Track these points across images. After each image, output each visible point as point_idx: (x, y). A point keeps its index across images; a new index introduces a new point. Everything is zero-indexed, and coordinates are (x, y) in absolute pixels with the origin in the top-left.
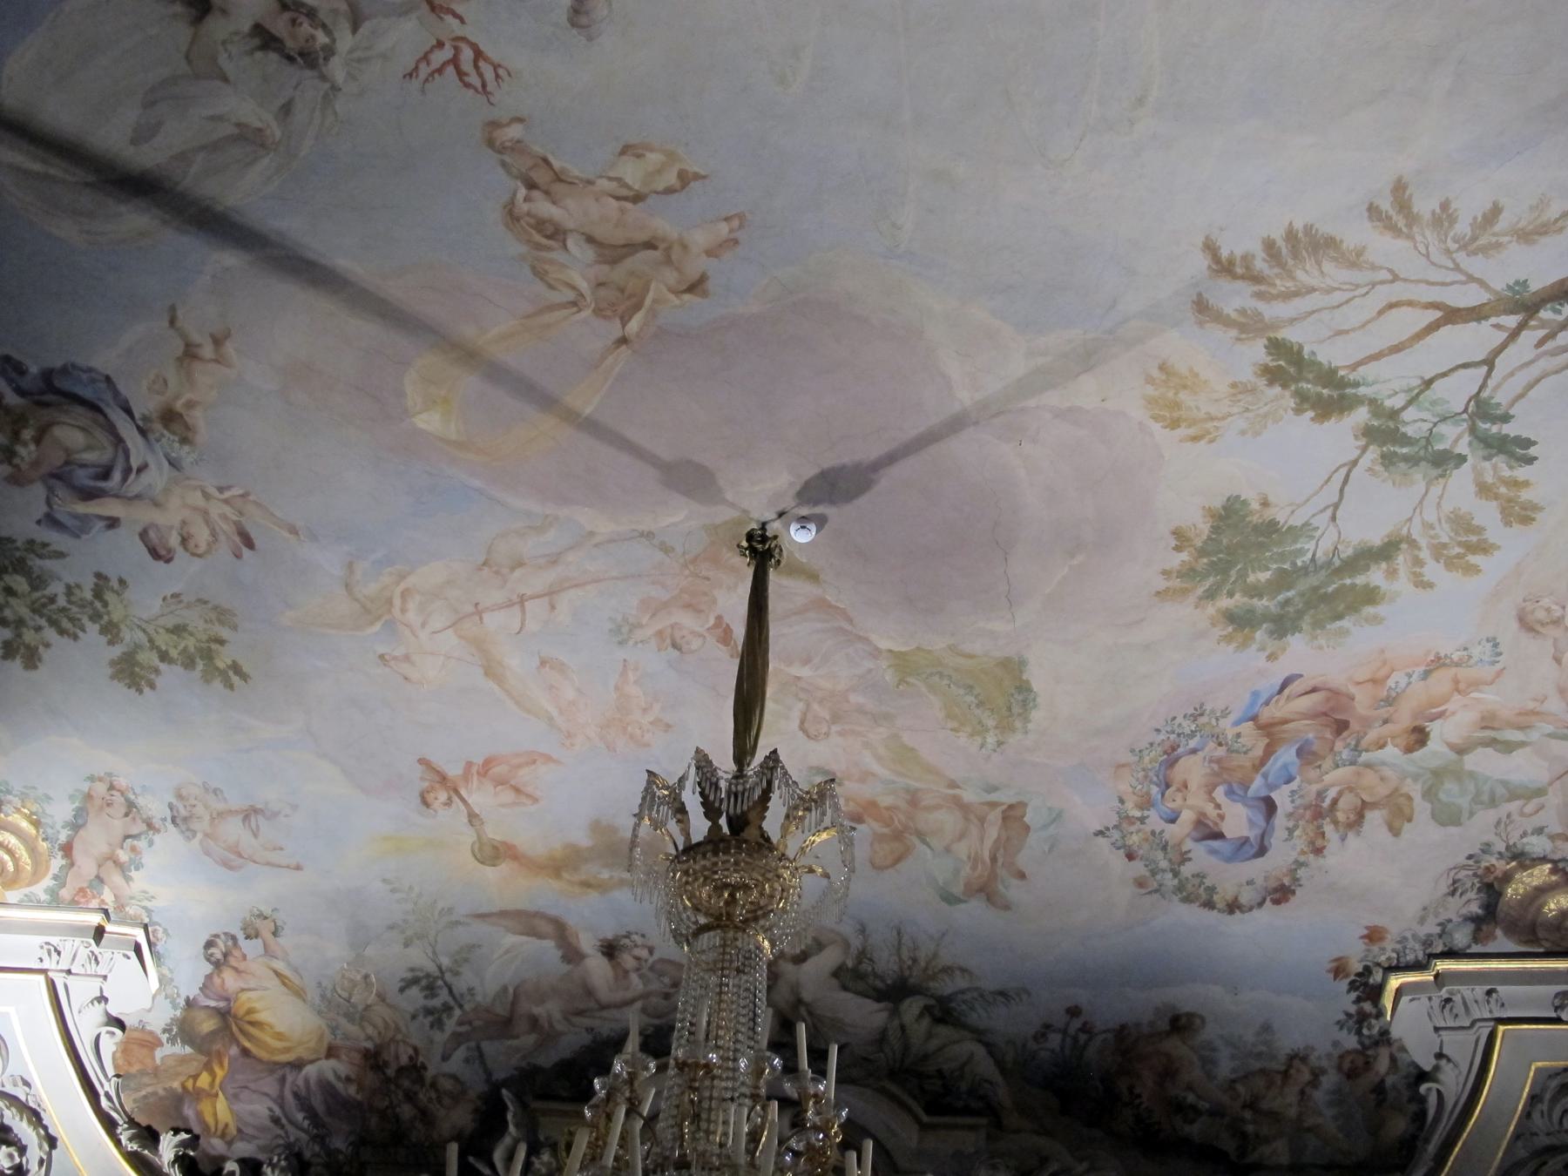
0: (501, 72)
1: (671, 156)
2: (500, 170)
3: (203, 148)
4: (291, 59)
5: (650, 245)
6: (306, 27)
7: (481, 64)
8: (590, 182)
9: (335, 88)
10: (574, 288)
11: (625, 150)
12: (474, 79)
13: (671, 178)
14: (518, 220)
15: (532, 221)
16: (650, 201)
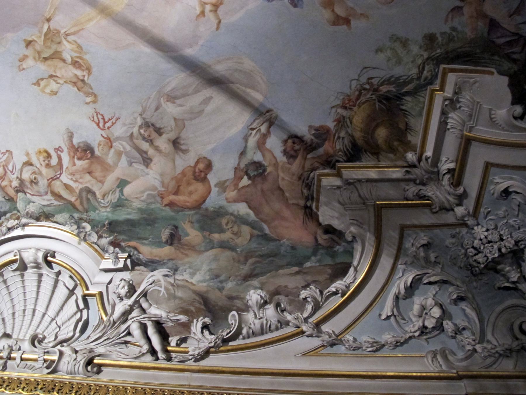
0: (92, 119)
1: (43, 91)
2: (92, 85)
3: (188, 95)
4: (153, 125)
5: (46, 59)
6: (146, 134)
7: (97, 122)
8: (65, 82)
9: (141, 115)
10: (68, 41)
11: (56, 93)
12: (100, 117)
13: (42, 83)
14: (87, 69)
15: (83, 68)
16: (46, 76)
